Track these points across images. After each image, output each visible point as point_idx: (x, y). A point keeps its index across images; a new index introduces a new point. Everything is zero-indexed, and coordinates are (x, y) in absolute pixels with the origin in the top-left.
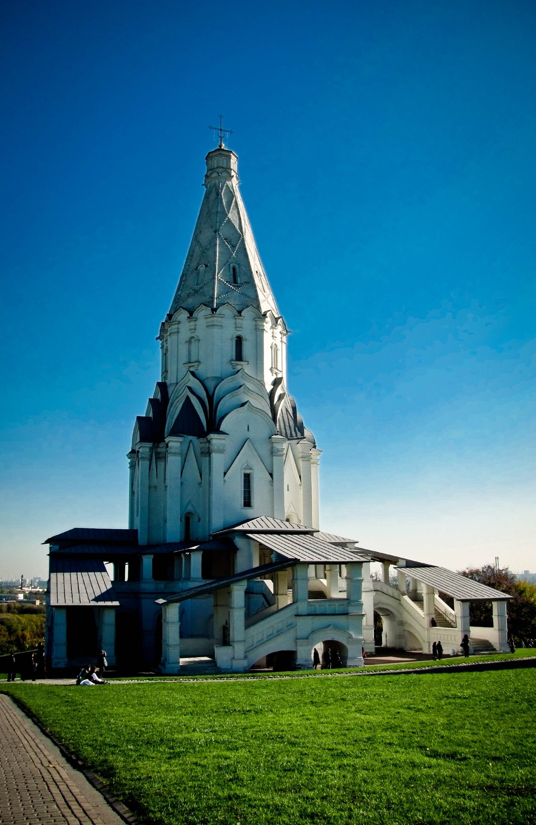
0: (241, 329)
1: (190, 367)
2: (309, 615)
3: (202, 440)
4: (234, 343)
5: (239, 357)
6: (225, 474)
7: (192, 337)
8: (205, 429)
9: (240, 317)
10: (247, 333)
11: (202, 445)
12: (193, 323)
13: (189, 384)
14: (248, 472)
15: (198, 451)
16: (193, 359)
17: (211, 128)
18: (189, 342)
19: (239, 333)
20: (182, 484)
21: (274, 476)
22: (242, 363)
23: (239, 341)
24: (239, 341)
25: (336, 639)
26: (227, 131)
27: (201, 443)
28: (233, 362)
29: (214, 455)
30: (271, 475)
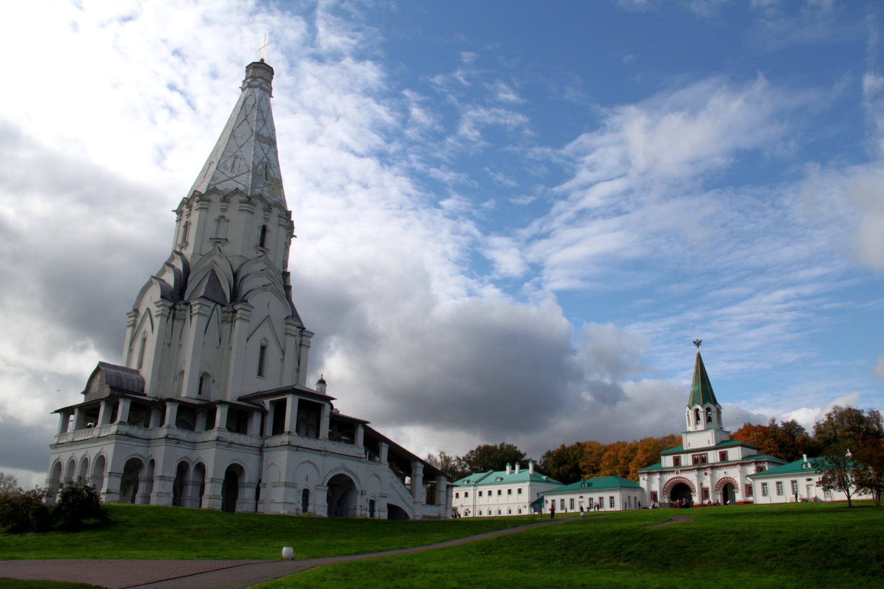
3: (225, 309)
4: (260, 231)
7: (223, 217)
8: (229, 301)
10: (271, 226)
11: (225, 314)
12: (225, 204)
13: (216, 258)
15: (220, 319)
19: (264, 223)
21: (286, 355)
23: (264, 230)
24: (264, 230)
27: (224, 312)
29: (238, 323)
30: (283, 352)
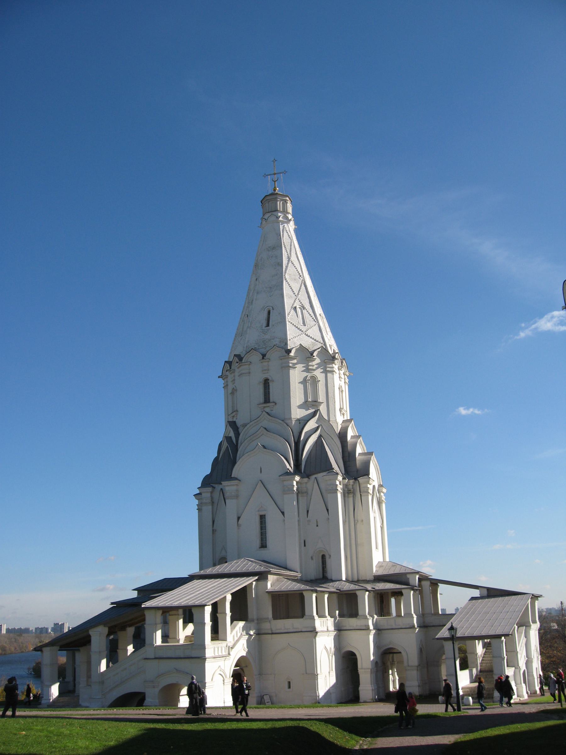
0: (266, 371)
1: (233, 417)
2: (156, 658)
5: (267, 400)
6: (239, 518)
9: (264, 360)
10: (273, 374)
14: (262, 513)
16: (235, 409)
17: (266, 175)
18: (232, 393)
19: (266, 376)
20: (214, 531)
22: (268, 405)
23: (266, 383)
24: (266, 383)
25: (170, 682)
26: (280, 173)
28: (260, 406)
30: (283, 513)
